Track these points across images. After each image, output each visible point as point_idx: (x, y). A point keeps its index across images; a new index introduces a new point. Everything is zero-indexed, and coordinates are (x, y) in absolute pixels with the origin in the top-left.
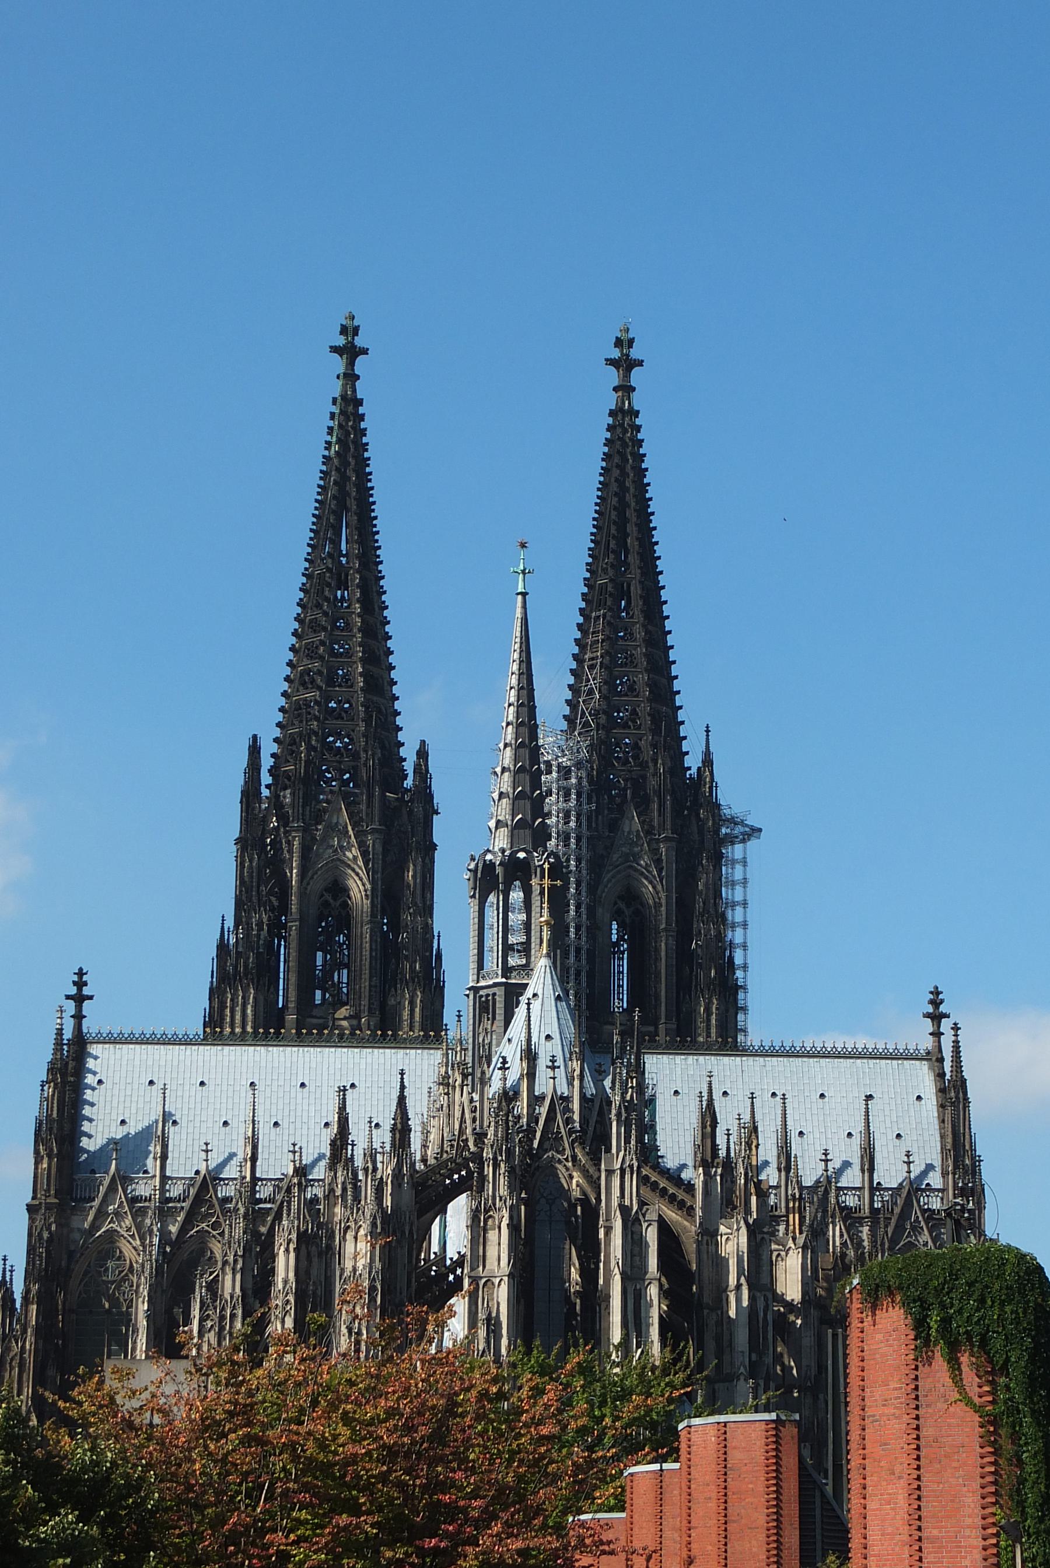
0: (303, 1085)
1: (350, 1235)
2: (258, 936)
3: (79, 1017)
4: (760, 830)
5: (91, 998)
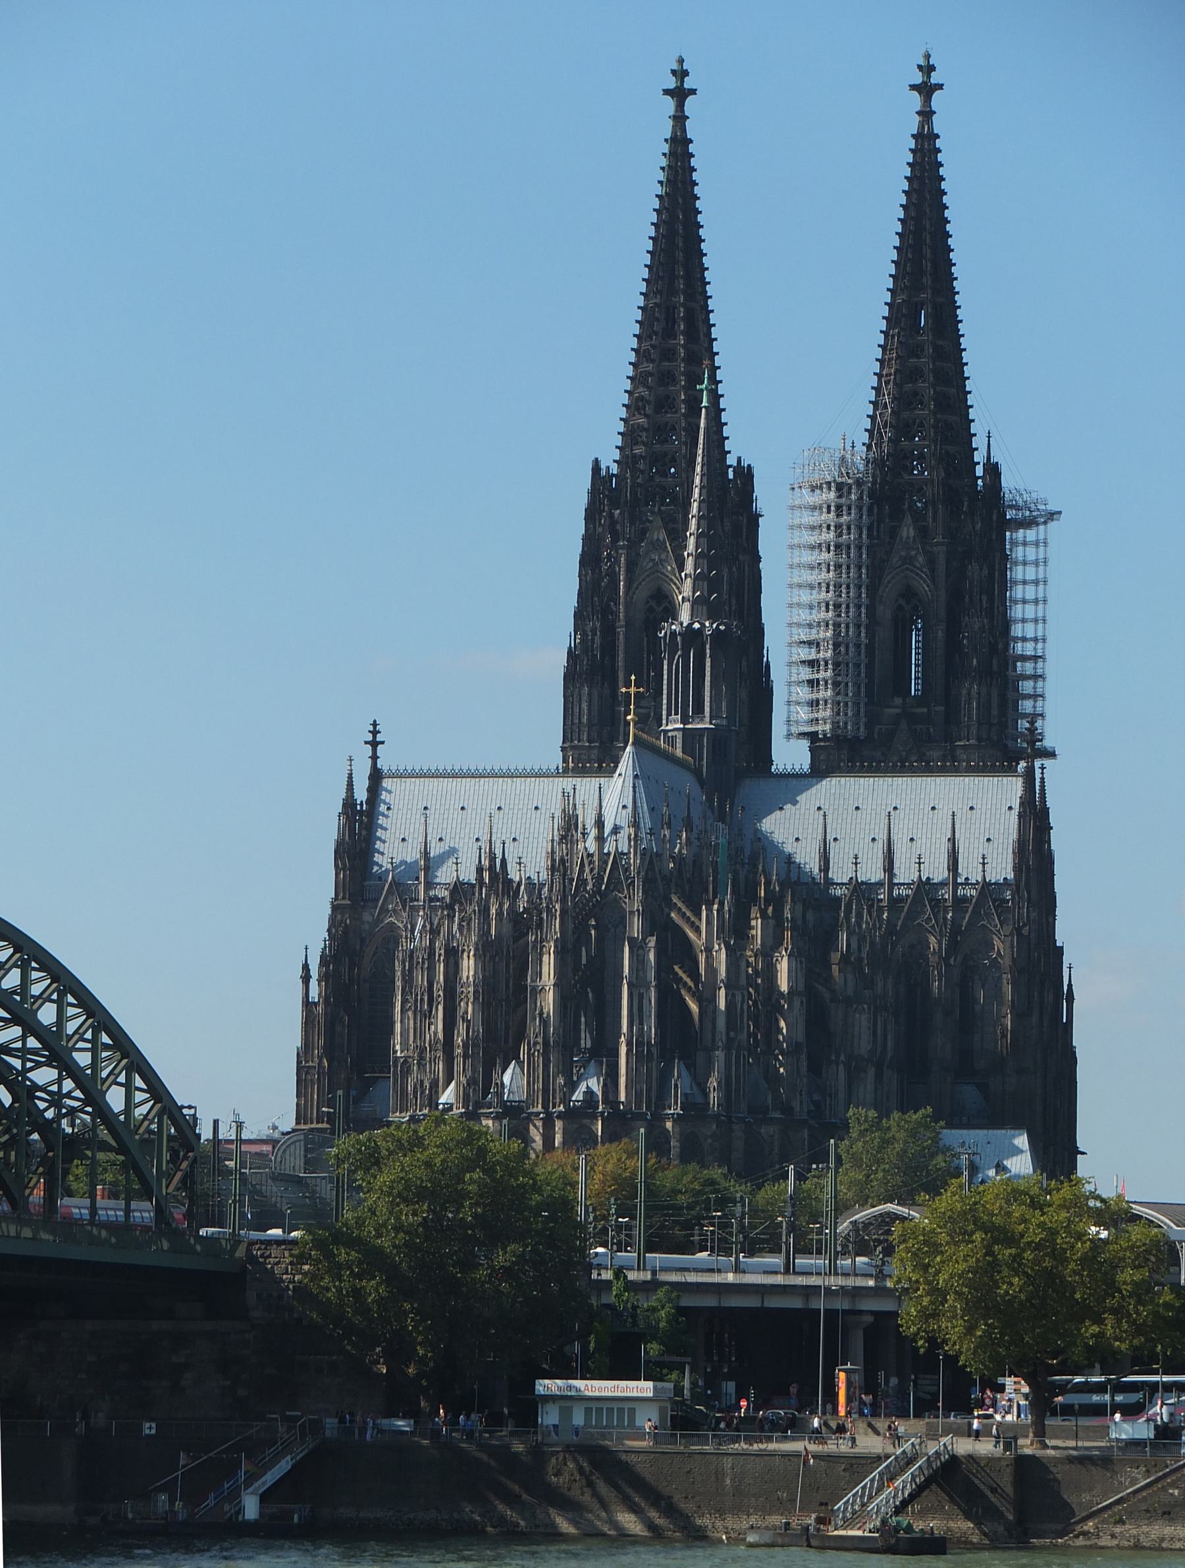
0: (536, 808)
1: (465, 954)
2: (593, 640)
3: (374, 758)
4: (1060, 513)
5: (383, 743)
